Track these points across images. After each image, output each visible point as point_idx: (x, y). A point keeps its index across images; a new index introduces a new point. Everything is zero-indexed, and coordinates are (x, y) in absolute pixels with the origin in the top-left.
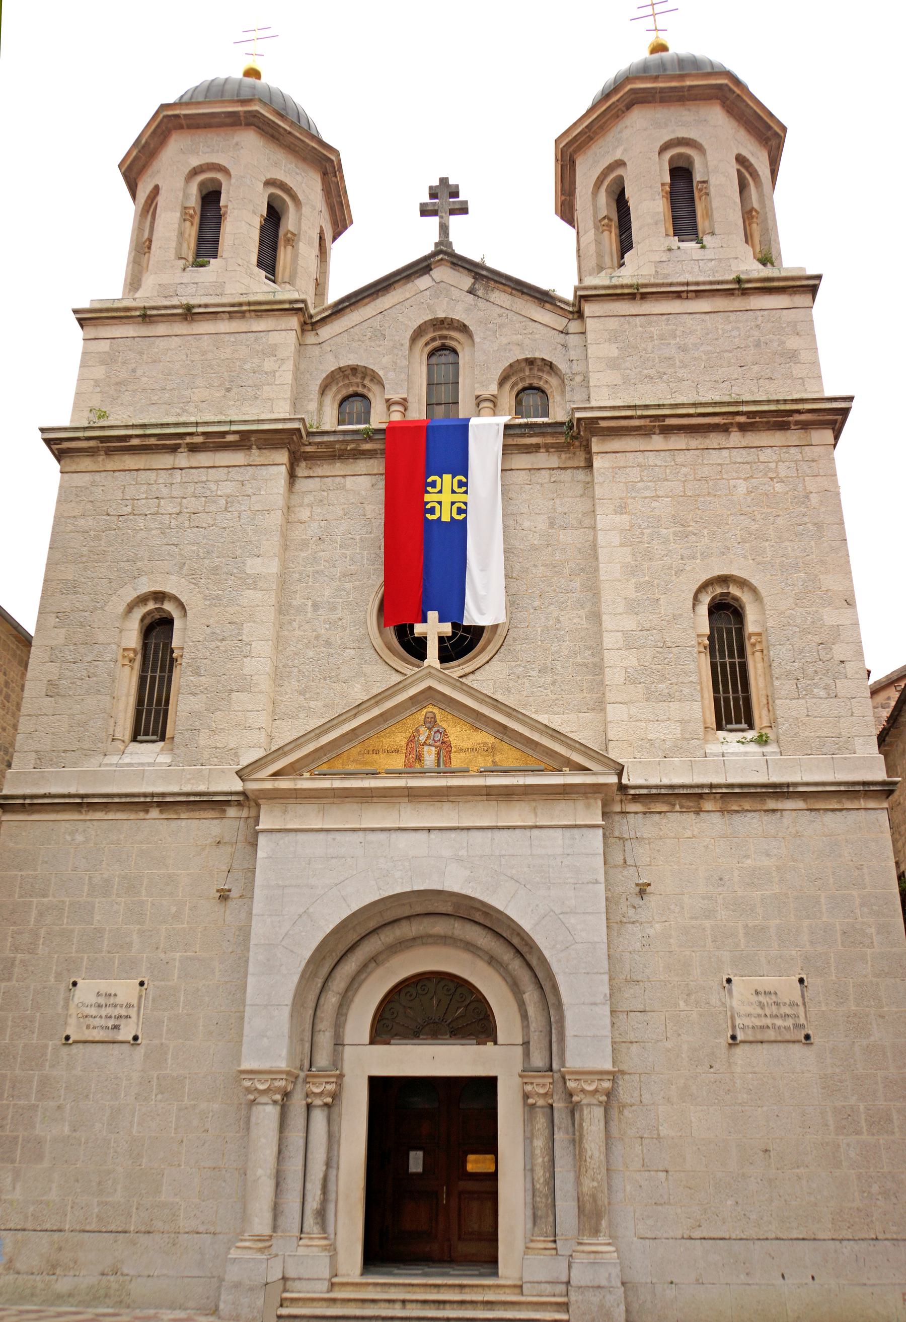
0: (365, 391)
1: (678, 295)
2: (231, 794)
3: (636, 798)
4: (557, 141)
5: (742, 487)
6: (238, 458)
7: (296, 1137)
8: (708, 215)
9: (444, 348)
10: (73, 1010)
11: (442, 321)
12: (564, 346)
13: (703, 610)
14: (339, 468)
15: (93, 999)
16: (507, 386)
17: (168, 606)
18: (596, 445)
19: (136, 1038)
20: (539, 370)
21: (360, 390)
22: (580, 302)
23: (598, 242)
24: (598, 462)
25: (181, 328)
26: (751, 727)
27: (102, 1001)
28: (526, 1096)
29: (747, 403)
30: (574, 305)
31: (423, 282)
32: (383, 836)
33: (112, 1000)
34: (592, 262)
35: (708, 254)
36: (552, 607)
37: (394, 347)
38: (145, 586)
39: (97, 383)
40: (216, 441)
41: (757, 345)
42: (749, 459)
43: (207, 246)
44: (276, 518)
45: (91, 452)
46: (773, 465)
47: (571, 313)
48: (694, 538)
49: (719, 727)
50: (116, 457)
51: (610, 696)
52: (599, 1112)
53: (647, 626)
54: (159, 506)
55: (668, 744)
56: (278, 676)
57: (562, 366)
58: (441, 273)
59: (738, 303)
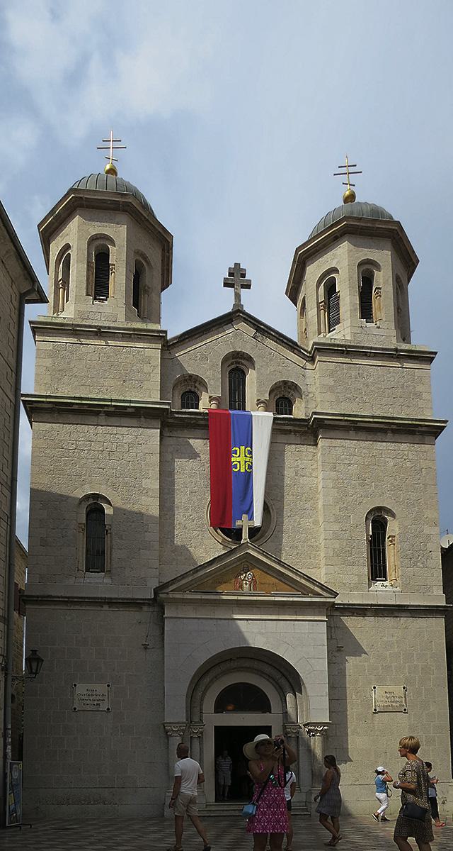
2: (145, 599)
11: (238, 353)
20: (289, 388)
22: (314, 351)
37: (213, 366)
47: (308, 357)
50: (64, 415)
55: (352, 586)
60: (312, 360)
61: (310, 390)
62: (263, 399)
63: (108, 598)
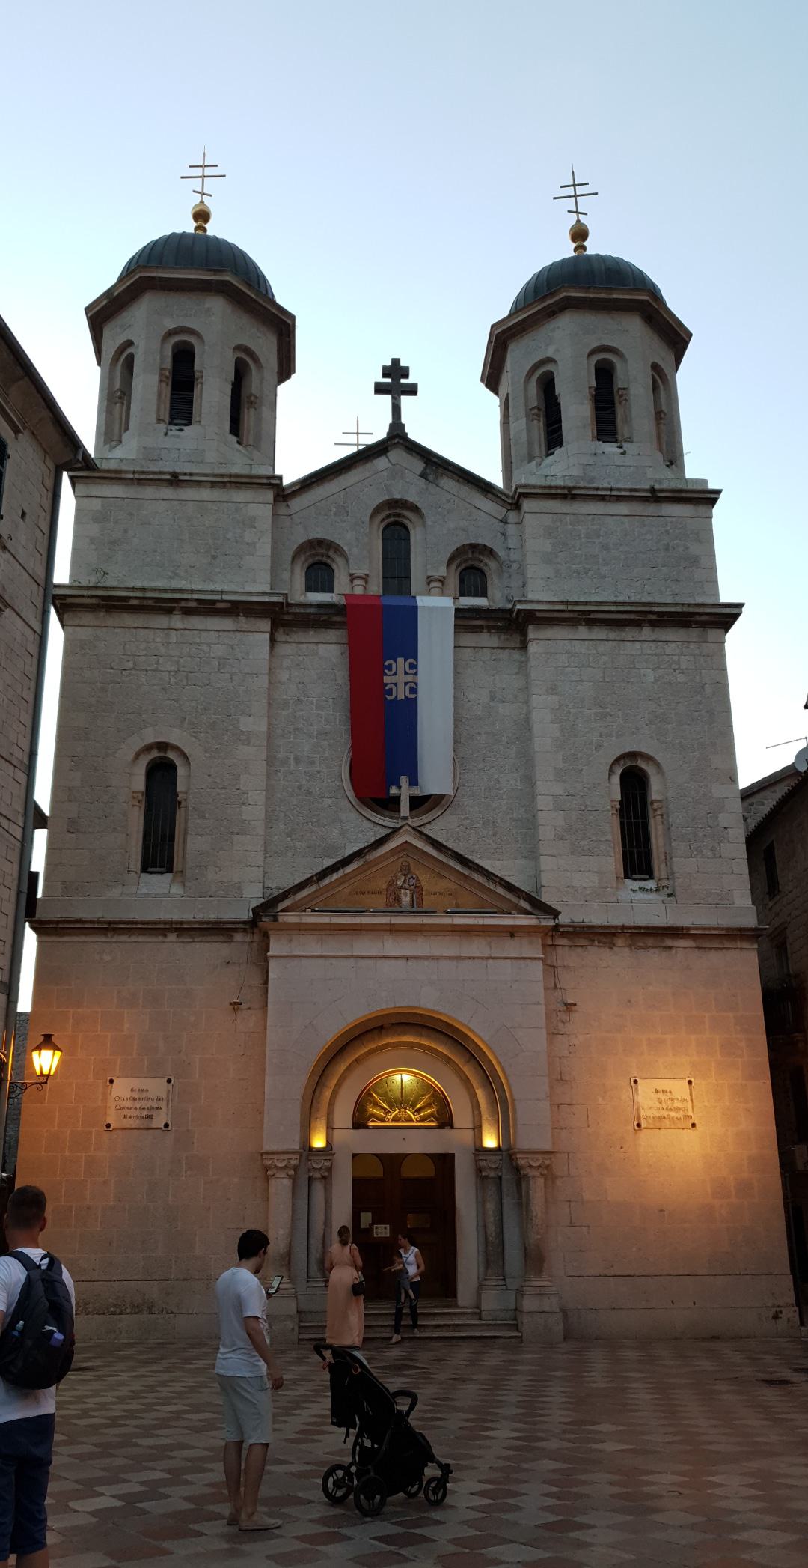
0: (329, 561)
1: (602, 498)
3: (563, 934)
4: (493, 327)
5: (650, 676)
6: (227, 623)
7: (303, 1204)
8: (627, 420)
9: (396, 523)
10: (112, 1104)
12: (504, 534)
13: (616, 779)
14: (312, 636)
15: (128, 1094)
16: (453, 566)
17: (171, 755)
18: (532, 633)
19: (166, 1126)
21: (324, 559)
23: (529, 430)
24: (533, 648)
25: (168, 493)
26: (651, 877)
27: (136, 1095)
28: (479, 1170)
29: (659, 604)
30: (513, 498)
31: (381, 463)
32: (371, 962)
33: (144, 1095)
34: (519, 451)
35: (628, 460)
36: (493, 770)
38: (151, 737)
39: (92, 541)
40: (208, 608)
41: (667, 549)
42: (658, 651)
43: (181, 405)
44: (263, 681)
45: (93, 608)
46: (676, 658)
48: (609, 718)
49: (626, 877)
51: (543, 850)
52: (540, 1182)
53: (572, 792)
54: (158, 663)
56: (269, 820)
57: (501, 553)
58: (397, 455)
59: (651, 509)
60: (516, 506)
61: (514, 556)
62: (436, 575)
63: (177, 923)
